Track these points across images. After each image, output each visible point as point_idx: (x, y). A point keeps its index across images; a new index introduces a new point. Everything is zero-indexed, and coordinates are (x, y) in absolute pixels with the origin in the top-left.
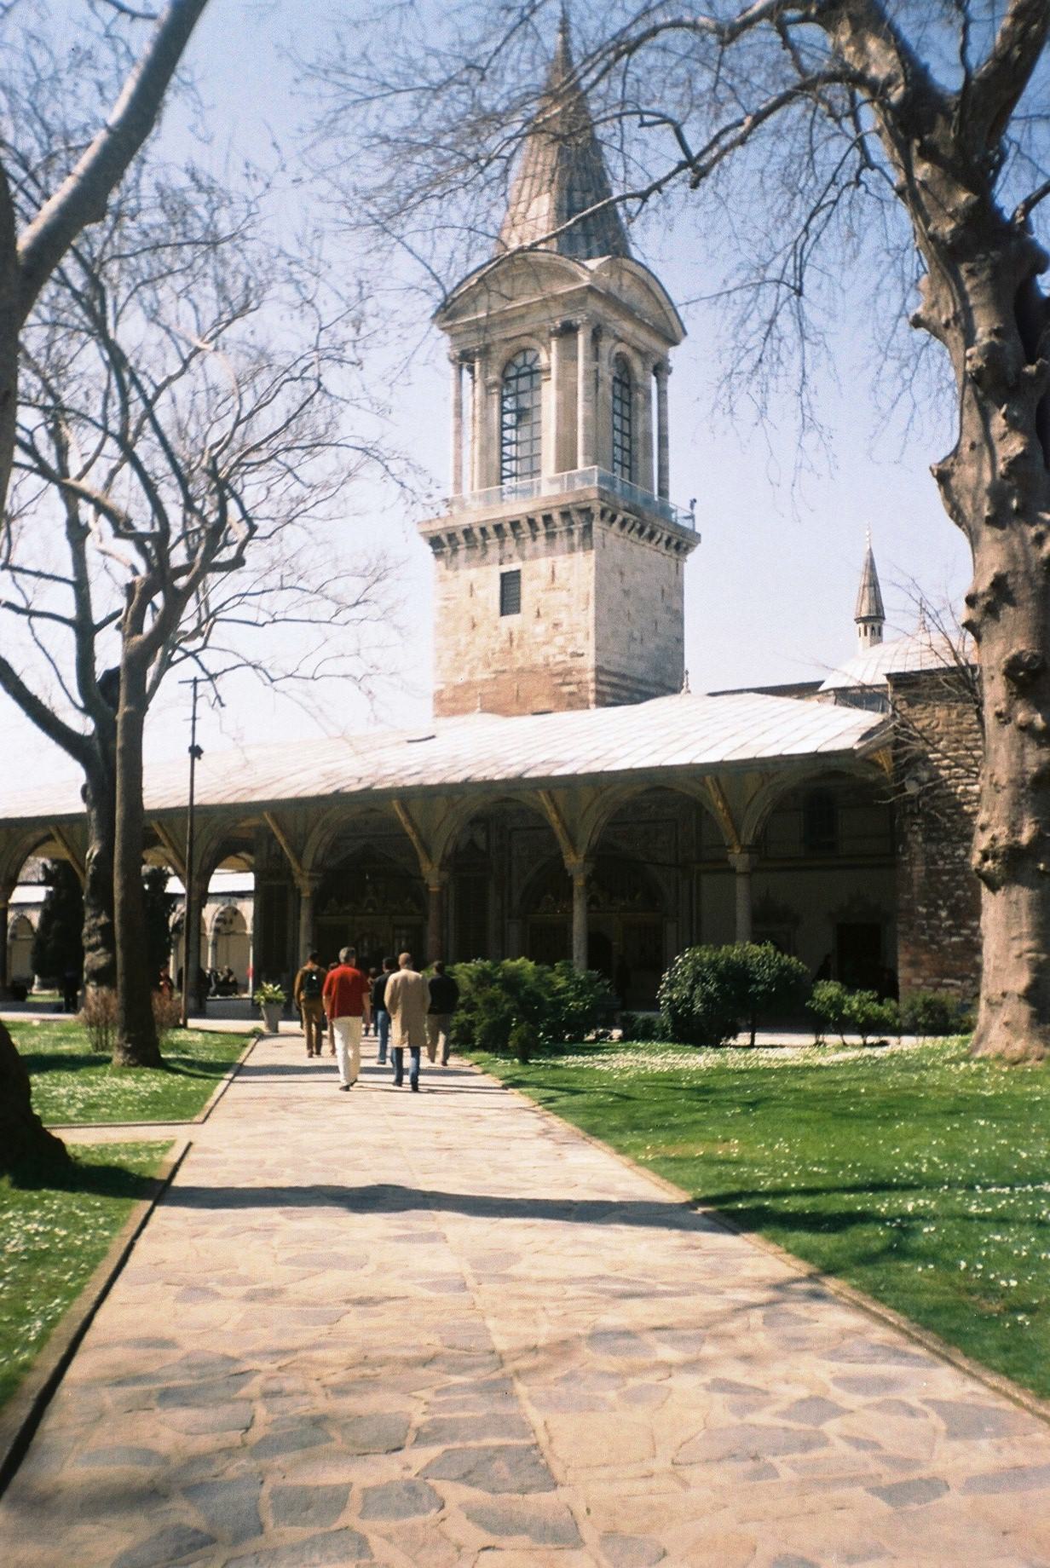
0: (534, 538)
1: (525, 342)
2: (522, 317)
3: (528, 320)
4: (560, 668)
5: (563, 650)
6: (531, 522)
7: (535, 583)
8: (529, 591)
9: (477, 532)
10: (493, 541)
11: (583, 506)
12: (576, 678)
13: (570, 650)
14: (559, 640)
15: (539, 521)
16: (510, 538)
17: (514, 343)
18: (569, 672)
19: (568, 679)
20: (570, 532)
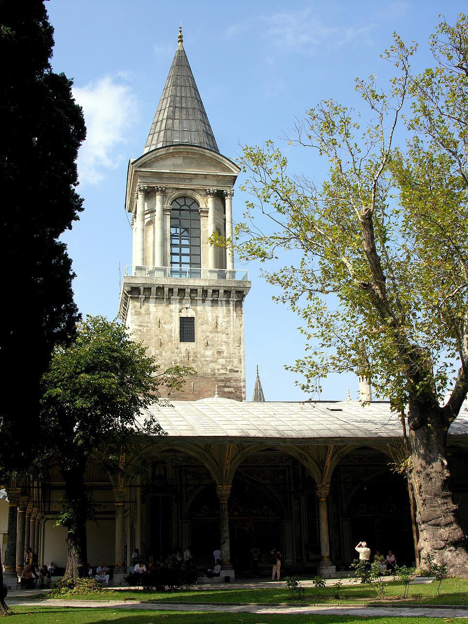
0: (204, 301)
1: (189, 193)
2: (191, 179)
3: (195, 182)
4: (223, 377)
5: (224, 367)
6: (205, 292)
7: (205, 327)
8: (199, 331)
9: (166, 289)
10: (175, 296)
11: (239, 289)
12: (234, 384)
13: (229, 368)
14: (222, 361)
15: (210, 291)
16: (187, 297)
17: (182, 192)
18: (229, 380)
19: (228, 384)
20: (228, 302)
